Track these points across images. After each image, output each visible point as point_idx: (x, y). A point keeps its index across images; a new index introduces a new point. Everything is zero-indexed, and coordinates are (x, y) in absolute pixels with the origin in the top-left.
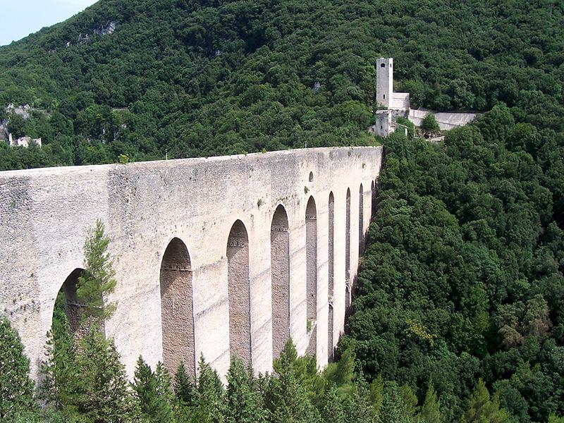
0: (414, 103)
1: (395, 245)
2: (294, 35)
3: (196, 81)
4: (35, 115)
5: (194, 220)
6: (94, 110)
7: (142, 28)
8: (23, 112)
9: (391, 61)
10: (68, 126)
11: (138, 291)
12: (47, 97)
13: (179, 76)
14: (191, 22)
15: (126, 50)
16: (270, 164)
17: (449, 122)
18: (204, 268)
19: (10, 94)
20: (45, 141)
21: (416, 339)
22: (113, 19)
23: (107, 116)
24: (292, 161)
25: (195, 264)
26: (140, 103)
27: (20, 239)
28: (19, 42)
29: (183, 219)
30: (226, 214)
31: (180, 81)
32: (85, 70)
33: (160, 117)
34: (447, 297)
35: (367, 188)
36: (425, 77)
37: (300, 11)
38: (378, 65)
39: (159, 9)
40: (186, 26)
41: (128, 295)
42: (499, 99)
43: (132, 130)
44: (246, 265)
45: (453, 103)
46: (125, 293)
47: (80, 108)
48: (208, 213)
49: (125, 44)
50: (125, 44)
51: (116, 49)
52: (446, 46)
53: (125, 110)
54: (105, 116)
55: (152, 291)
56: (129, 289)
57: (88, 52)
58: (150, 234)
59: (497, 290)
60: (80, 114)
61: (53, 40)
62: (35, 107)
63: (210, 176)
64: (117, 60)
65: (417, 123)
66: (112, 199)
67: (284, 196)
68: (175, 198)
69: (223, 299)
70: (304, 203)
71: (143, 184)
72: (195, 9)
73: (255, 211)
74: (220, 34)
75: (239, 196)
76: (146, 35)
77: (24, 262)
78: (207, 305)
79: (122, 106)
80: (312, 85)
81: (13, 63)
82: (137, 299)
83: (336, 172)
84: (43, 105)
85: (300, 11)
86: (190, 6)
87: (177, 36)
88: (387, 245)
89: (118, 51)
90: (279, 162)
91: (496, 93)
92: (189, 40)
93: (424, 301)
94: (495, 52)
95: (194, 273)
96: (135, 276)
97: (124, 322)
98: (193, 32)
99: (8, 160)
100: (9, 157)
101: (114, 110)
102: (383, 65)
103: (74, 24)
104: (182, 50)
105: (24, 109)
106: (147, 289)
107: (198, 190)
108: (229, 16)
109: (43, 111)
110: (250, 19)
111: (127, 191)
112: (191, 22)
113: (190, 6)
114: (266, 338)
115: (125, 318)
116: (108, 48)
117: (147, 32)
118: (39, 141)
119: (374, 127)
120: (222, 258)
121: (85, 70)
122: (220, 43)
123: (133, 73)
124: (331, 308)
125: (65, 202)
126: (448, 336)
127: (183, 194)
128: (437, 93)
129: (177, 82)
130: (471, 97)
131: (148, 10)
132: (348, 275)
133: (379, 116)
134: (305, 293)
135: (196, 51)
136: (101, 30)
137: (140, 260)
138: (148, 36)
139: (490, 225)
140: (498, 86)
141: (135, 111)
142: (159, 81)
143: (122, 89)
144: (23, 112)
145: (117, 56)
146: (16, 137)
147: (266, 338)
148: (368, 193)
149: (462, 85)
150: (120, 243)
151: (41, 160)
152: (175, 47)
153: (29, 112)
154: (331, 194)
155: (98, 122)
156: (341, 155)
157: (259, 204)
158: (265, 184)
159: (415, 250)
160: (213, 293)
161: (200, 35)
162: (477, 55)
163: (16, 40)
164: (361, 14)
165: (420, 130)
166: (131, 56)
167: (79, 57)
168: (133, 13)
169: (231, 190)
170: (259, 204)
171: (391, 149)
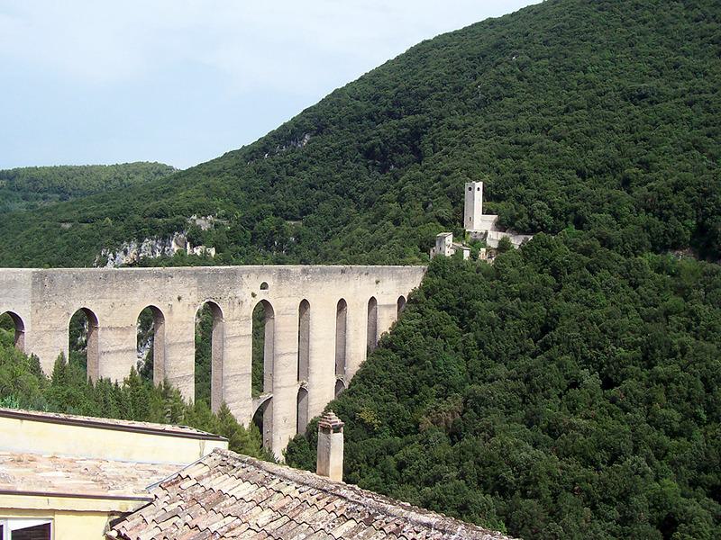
0: (500, 226)
1: (394, 350)
3: (362, 197)
4: (216, 226)
5: (102, 300)
6: (270, 222)
8: (204, 224)
9: (480, 185)
10: (245, 237)
12: (231, 209)
13: (352, 190)
14: (374, 135)
15: (312, 163)
16: (196, 274)
17: (516, 241)
18: (111, 328)
19: (195, 205)
21: (362, 421)
22: (307, 131)
24: (235, 273)
26: (312, 216)
29: (93, 298)
32: (274, 180)
33: (326, 230)
34: (409, 394)
36: (520, 199)
37: (456, 128)
38: (466, 189)
39: (351, 120)
40: (369, 139)
43: (299, 242)
45: (530, 225)
47: (258, 220)
49: (313, 157)
50: (313, 157)
52: (557, 166)
54: (278, 228)
59: (446, 392)
60: (258, 224)
61: (253, 151)
62: (218, 218)
63: (119, 277)
65: (494, 245)
66: (34, 284)
68: (86, 287)
71: (59, 280)
72: (382, 122)
73: (175, 303)
74: (394, 148)
78: (113, 349)
79: (296, 219)
84: (226, 216)
85: (456, 128)
86: (379, 118)
87: (360, 150)
88: (389, 351)
91: (571, 216)
92: (369, 154)
93: (392, 395)
98: (374, 146)
102: (470, 189)
103: (274, 136)
104: (361, 165)
107: (107, 285)
108: (404, 130)
109: (225, 222)
110: (424, 133)
111: (46, 281)
112: (374, 135)
113: (379, 118)
116: (298, 161)
117: (333, 145)
118: (213, 252)
121: (274, 180)
122: (395, 158)
123: (312, 187)
124: (302, 392)
126: (391, 423)
127: (93, 286)
128: (521, 216)
129: (351, 196)
130: (549, 220)
131: (340, 122)
135: (374, 164)
137: (54, 315)
138: (334, 149)
139: (476, 339)
140: (576, 209)
143: (298, 202)
144: (204, 224)
145: (305, 169)
146: (193, 246)
148: (389, 306)
149: (540, 208)
155: (272, 233)
156: (330, 272)
157: (179, 299)
158: (189, 286)
159: (405, 356)
162: (581, 174)
164: (500, 132)
165: (495, 252)
166: (315, 169)
167: (272, 169)
168: (326, 126)
169: (143, 288)
170: (179, 299)
171: (437, 268)
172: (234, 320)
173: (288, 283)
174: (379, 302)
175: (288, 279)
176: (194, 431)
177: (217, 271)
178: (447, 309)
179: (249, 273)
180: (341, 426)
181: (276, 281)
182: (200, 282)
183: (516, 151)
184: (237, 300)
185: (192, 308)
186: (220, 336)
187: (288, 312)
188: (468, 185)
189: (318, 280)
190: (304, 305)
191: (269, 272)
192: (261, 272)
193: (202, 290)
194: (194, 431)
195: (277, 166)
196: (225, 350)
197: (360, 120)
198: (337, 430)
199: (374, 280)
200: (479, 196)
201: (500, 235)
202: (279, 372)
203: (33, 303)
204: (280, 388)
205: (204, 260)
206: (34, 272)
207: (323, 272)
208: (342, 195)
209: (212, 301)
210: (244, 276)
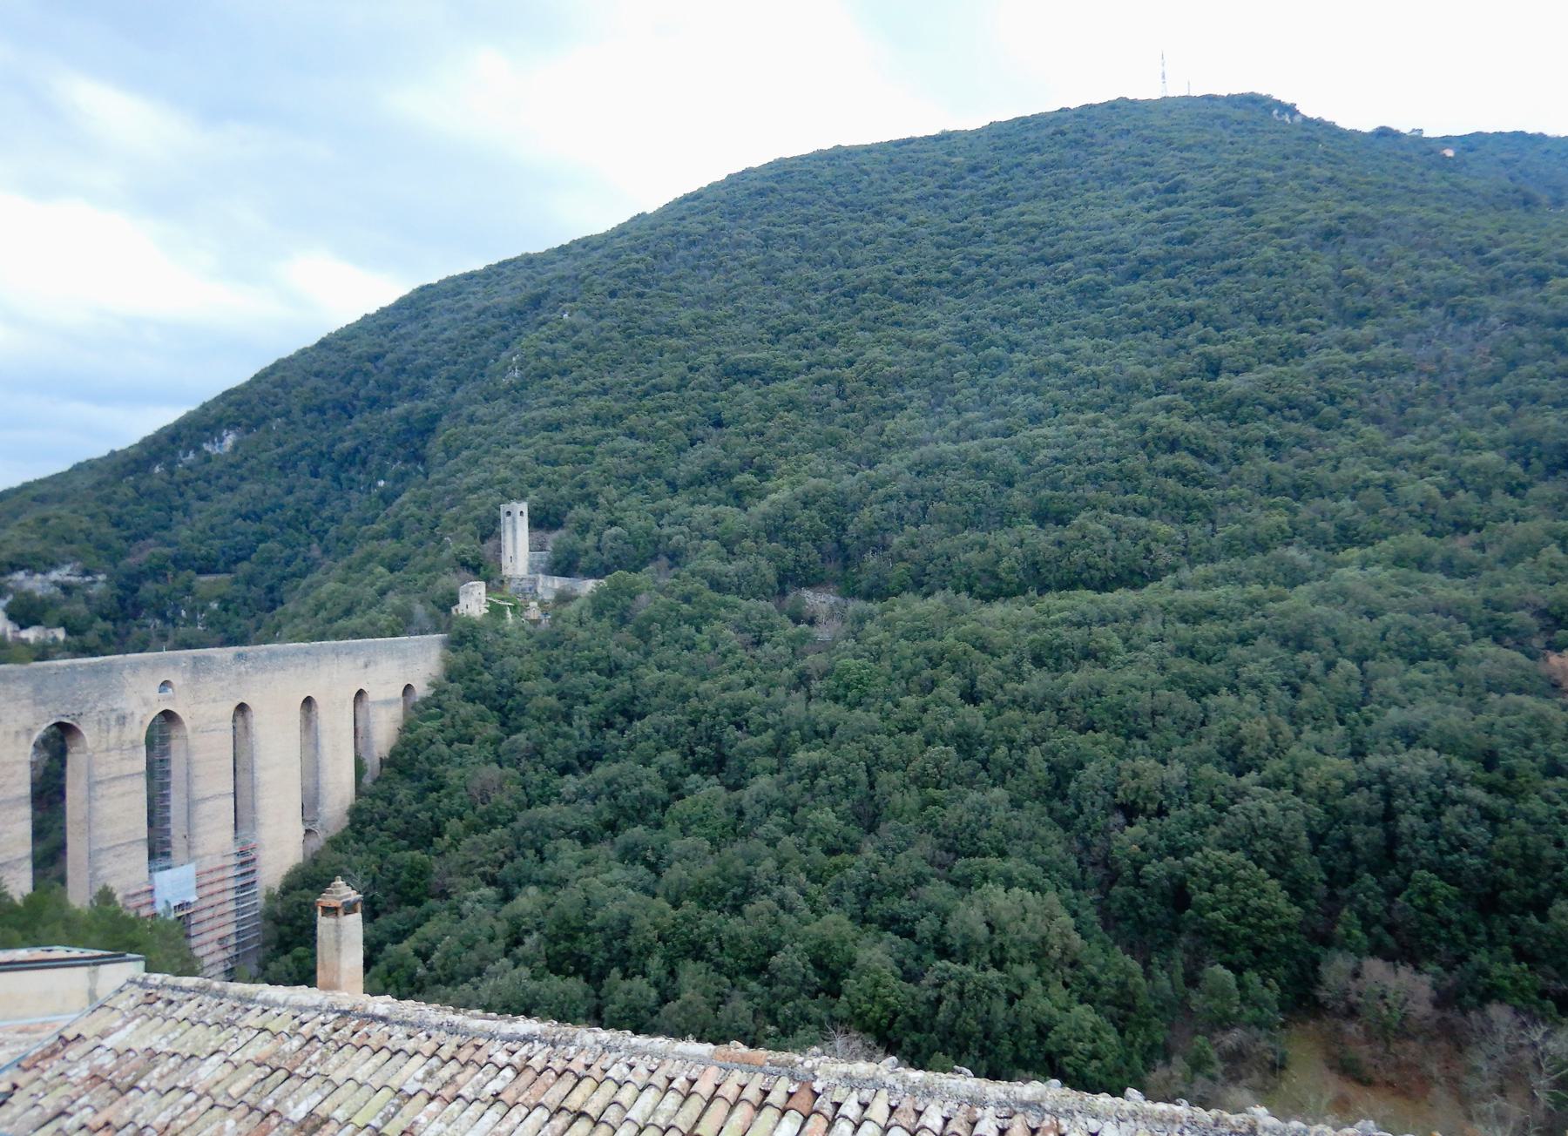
9: (524, 506)
15: (242, 479)
22: (235, 425)
38: (502, 515)
57: (186, 483)
101: (204, 578)
102: (509, 513)
118: (60, 634)
145: (231, 489)
148: (388, 703)
158: (16, 699)
172: (108, 750)
173: (209, 679)
174: (373, 695)
175: (208, 671)
176: (75, 953)
177: (73, 667)
178: (483, 700)
179: (135, 668)
180: (355, 903)
181: (188, 676)
182: (38, 689)
184: (113, 717)
185: (23, 739)
186: (83, 781)
187: (213, 726)
188: (504, 508)
189: (264, 670)
190: (242, 708)
191: (175, 663)
192: (156, 666)
193: (44, 703)
194: (75, 953)
196: (97, 804)
197: (321, 410)
198: (350, 908)
199: (361, 662)
200: (523, 524)
201: (558, 583)
202: (199, 830)
205: (43, 652)
207: (272, 655)
209: (66, 720)
210: (126, 673)
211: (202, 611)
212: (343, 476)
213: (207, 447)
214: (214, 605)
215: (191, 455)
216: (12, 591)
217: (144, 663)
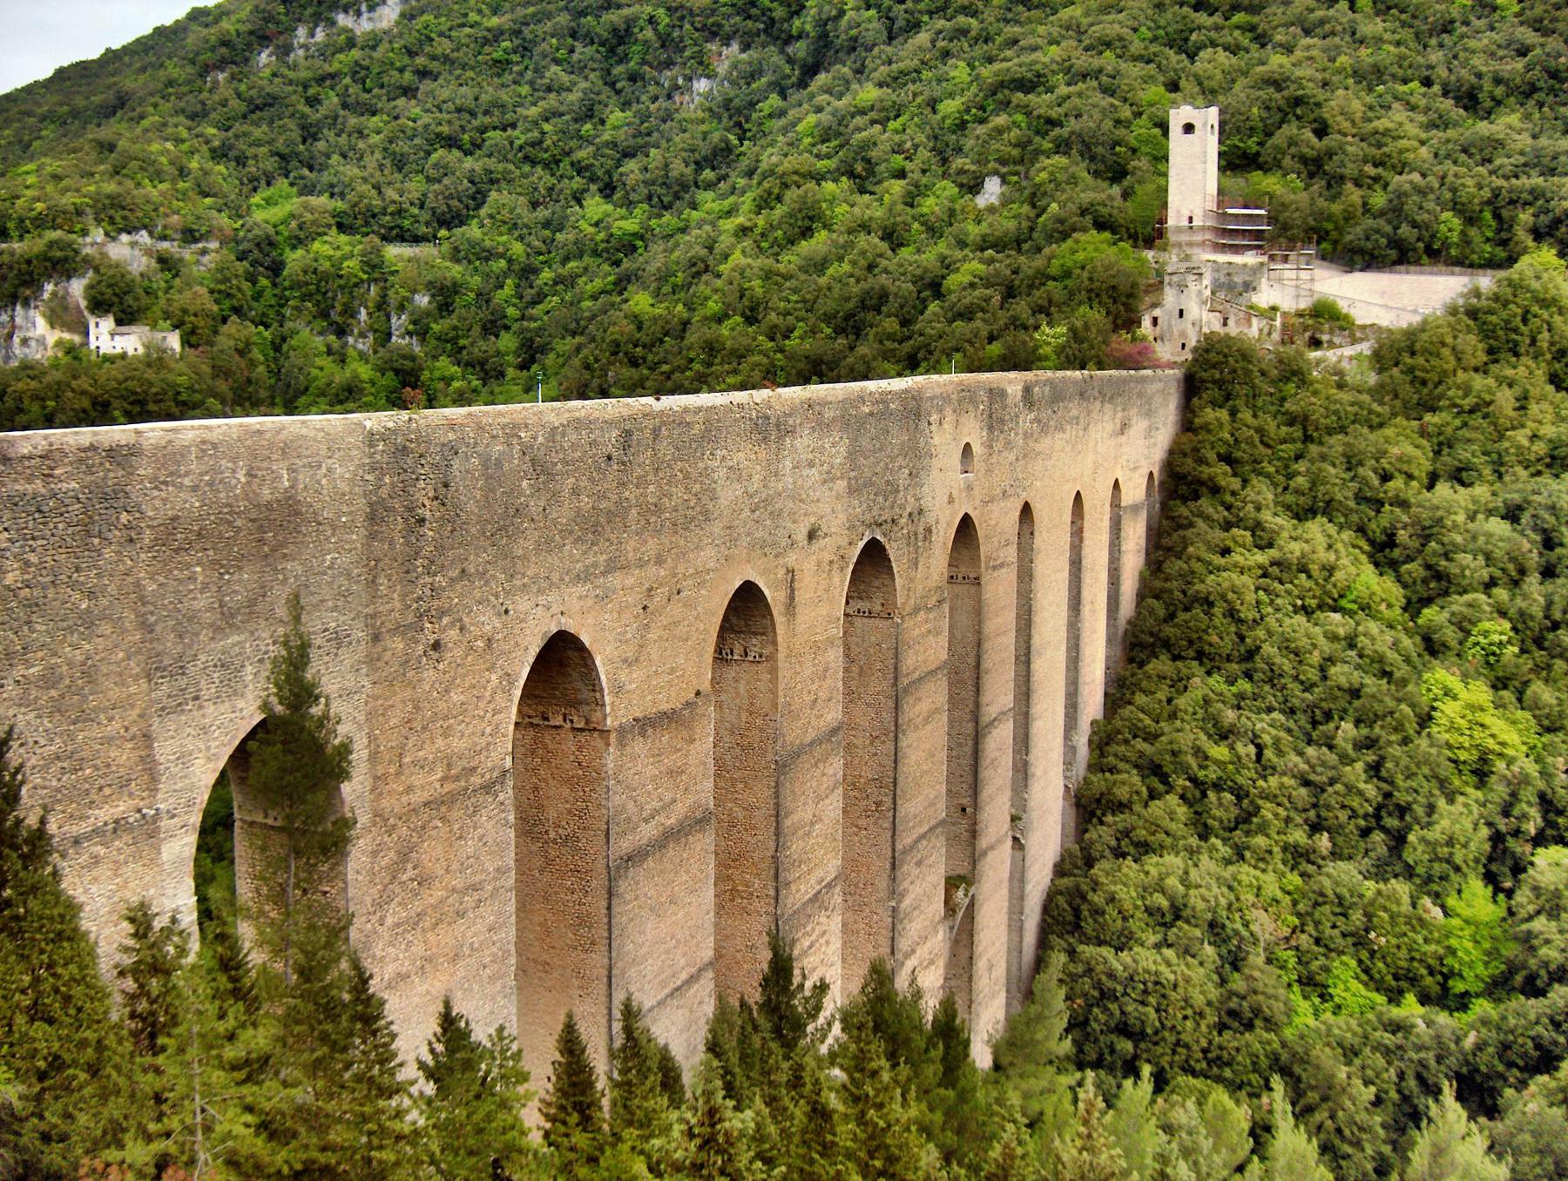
2: (923, 38)
4: (164, 261)
5: (615, 580)
7: (480, 12)
9: (1213, 114)
11: (448, 787)
15: (423, 74)
18: (644, 725)
20: (186, 342)
23: (374, 266)
24: (914, 411)
25: (616, 711)
27: (105, 628)
28: (126, 50)
30: (711, 565)
31: (588, 167)
35: (1135, 491)
36: (1314, 167)
41: (417, 798)
42: (1538, 235)
44: (729, 896)
46: (409, 789)
48: (660, 561)
49: (434, 58)
50: (434, 58)
51: (401, 70)
52: (1378, 73)
53: (425, 251)
55: (487, 788)
56: (418, 779)
57: (321, 80)
58: (488, 621)
64: (401, 102)
67: (886, 516)
69: (699, 815)
70: (945, 534)
75: (753, 511)
76: (489, 30)
77: (115, 693)
78: (648, 832)
79: (417, 240)
80: (975, 188)
81: (109, 111)
82: (443, 809)
83: (1045, 444)
89: (408, 75)
90: (871, 414)
91: (1525, 217)
94: (1529, 91)
95: (613, 737)
96: (440, 742)
97: (405, 878)
99: (84, 393)
100: (83, 383)
102: (1189, 128)
105: (133, 245)
106: (476, 780)
114: (824, 933)
115: (410, 866)
117: (495, 21)
118: (174, 341)
119: (1157, 312)
120: (698, 693)
123: (451, 142)
125: (239, 523)
130: (1450, 224)
132: (1070, 750)
133: (1175, 278)
134: (942, 804)
136: (359, 14)
137: (456, 697)
138: (497, 35)
140: (1536, 194)
141: (455, 254)
142: (527, 168)
145: (409, 92)
147: (824, 933)
148: (1135, 508)
150: (398, 644)
151: (178, 393)
152: (579, 69)
153: (148, 252)
154: (1026, 510)
156: (1058, 395)
157: (811, 536)
160: (668, 797)
161: (649, 34)
162: (1470, 100)
163: (116, 46)
166: (443, 89)
183: (1217, 28)
195: (306, 87)
203: (376, 638)
204: (985, 853)
206: (371, 438)
208: (551, 164)
211: (401, 308)
212: (618, 70)
213: (343, 20)
214: (423, 300)
215: (320, 35)
216: (87, 262)
217: (946, 399)
